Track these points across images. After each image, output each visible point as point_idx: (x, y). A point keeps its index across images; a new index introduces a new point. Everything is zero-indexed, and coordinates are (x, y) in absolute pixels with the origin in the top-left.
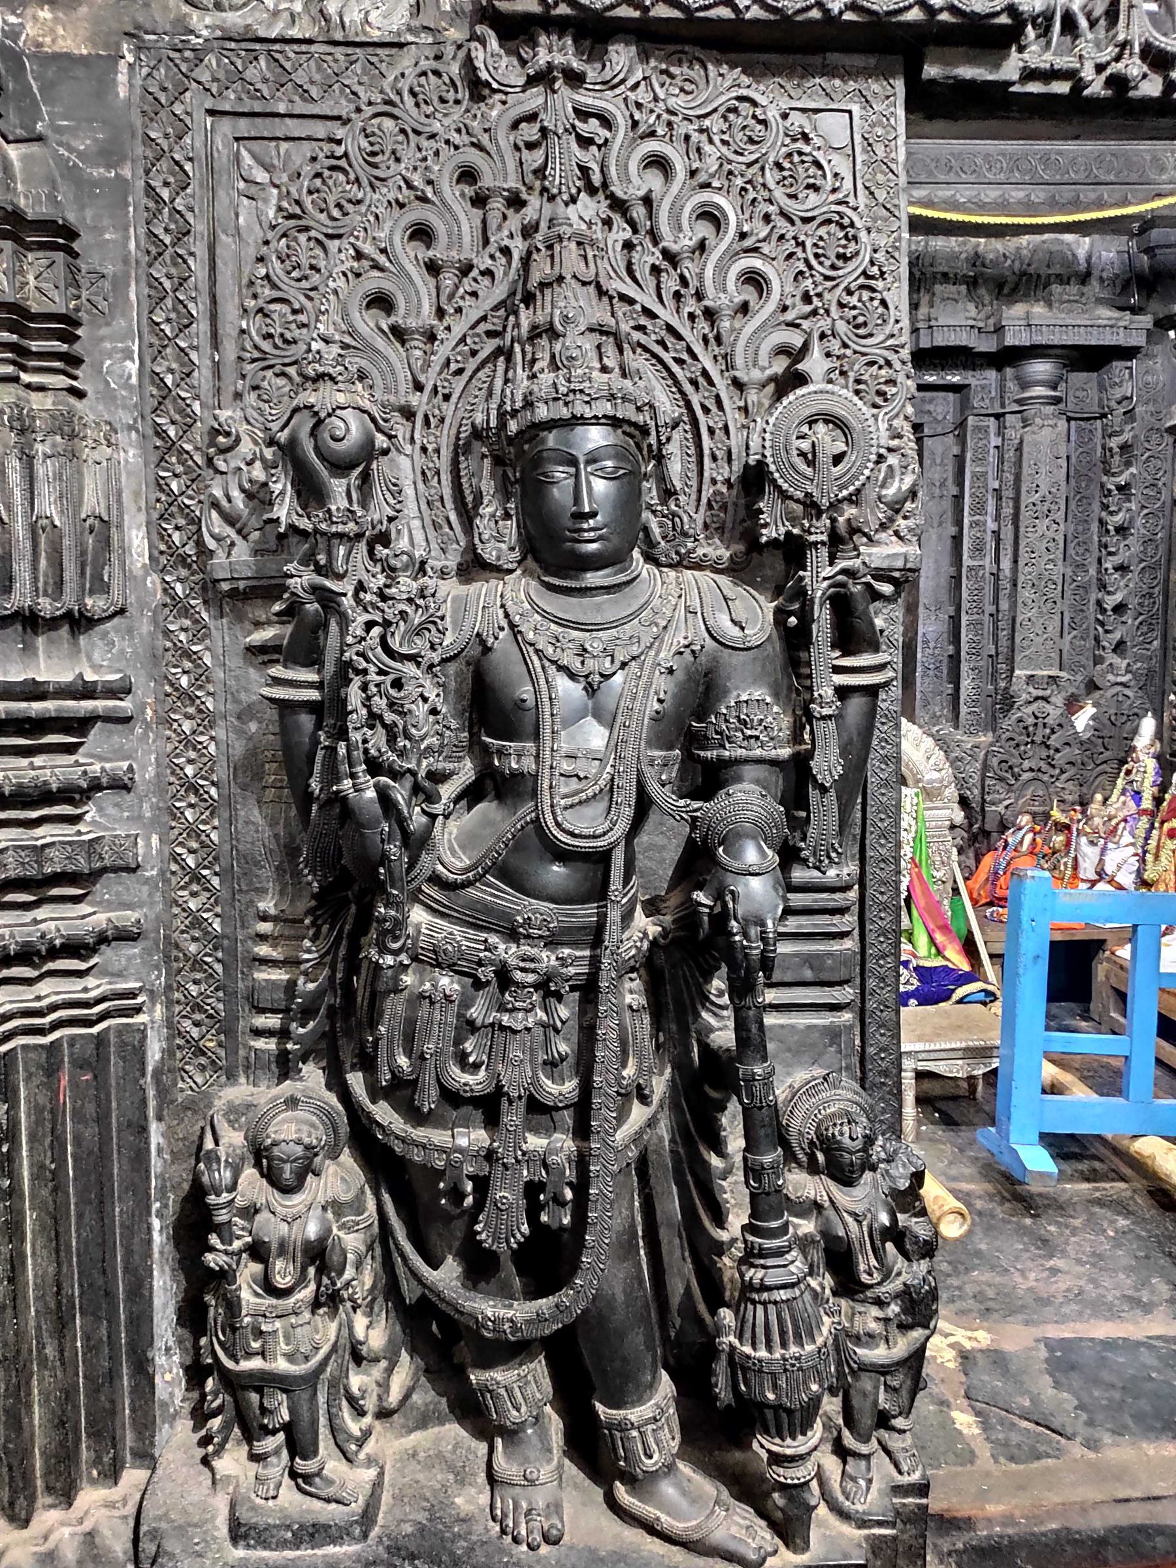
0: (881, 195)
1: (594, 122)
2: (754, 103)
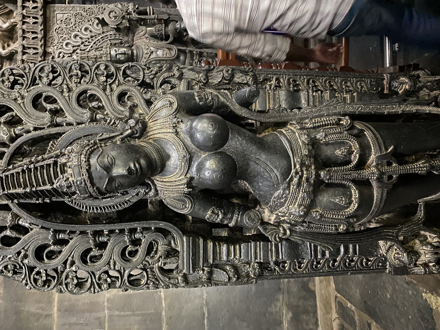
0: (70, 9)
1: (60, 55)
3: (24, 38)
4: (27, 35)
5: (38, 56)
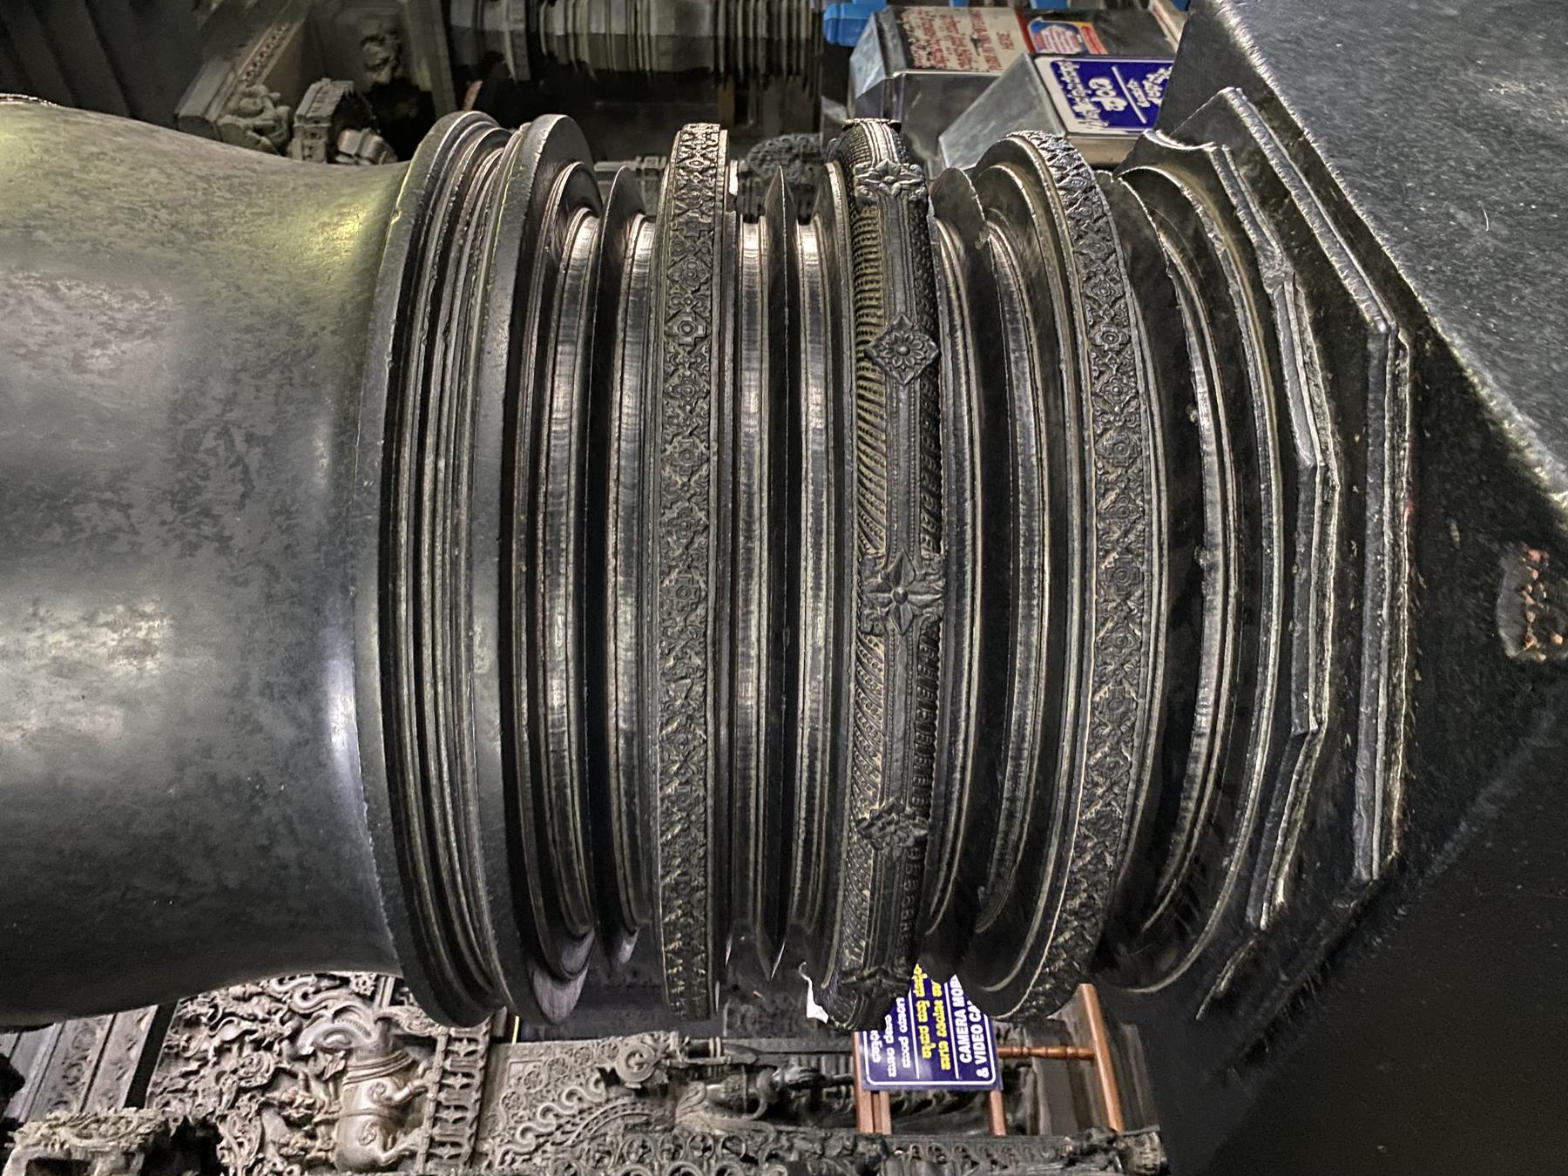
3: (435, 1120)
4: (444, 1114)
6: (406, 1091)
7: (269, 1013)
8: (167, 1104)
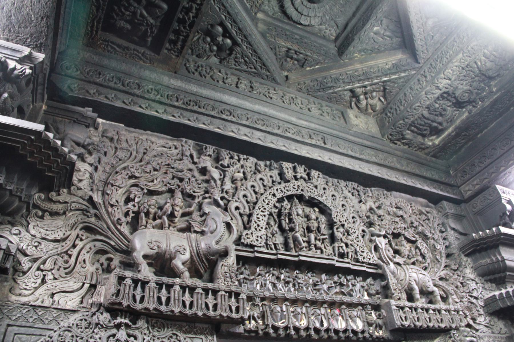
2: (177, 335)
5: (131, 303)
6: (181, 267)
7: (227, 192)
8: (176, 148)
